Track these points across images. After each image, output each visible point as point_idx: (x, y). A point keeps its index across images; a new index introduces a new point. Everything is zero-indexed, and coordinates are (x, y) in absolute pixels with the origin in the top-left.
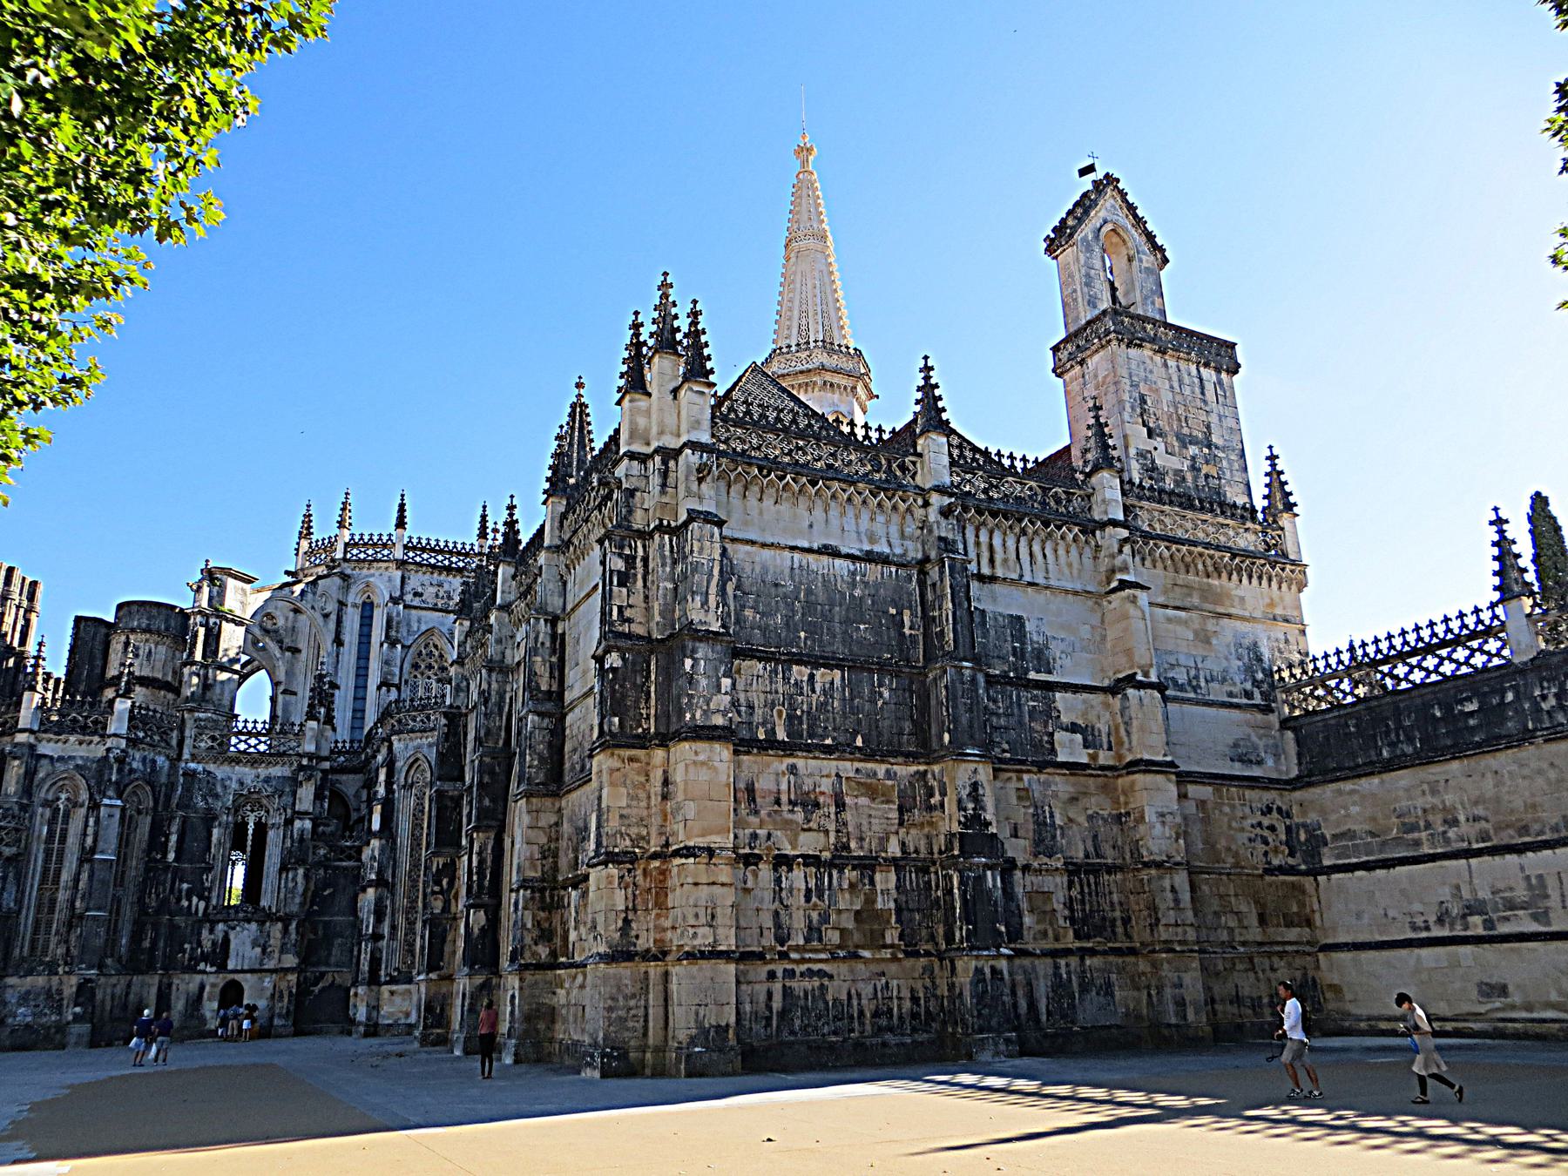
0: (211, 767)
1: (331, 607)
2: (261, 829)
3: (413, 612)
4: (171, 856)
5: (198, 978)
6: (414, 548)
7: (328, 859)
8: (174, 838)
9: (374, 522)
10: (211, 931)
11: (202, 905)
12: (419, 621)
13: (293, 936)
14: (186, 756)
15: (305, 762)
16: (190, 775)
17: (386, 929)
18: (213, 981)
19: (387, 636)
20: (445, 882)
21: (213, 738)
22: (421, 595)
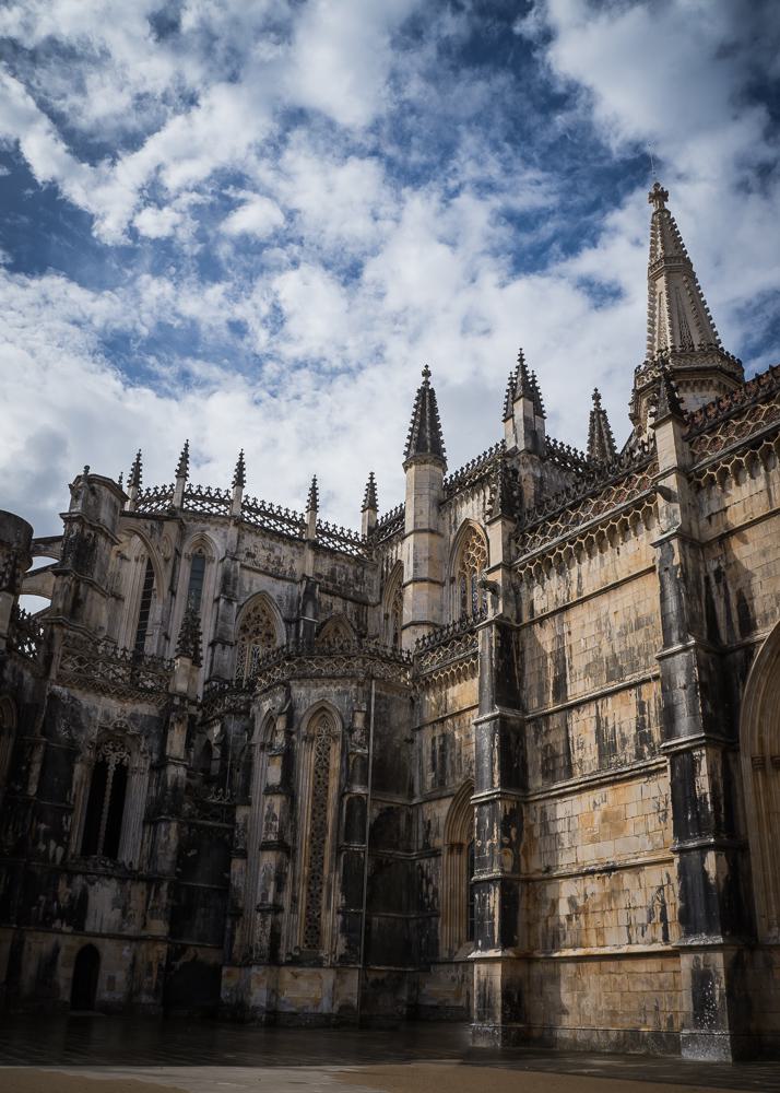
0: (77, 693)
1: (170, 553)
2: (123, 772)
3: (246, 572)
4: (33, 789)
5: (53, 938)
6: (250, 509)
7: (193, 817)
8: (36, 768)
9: (213, 476)
10: (69, 884)
11: (60, 851)
12: (251, 583)
13: (165, 899)
14: (53, 676)
15: (177, 701)
16: (54, 697)
17: (286, 901)
18: (69, 944)
19: (224, 590)
20: (513, 832)
21: (81, 661)
22: (254, 556)
